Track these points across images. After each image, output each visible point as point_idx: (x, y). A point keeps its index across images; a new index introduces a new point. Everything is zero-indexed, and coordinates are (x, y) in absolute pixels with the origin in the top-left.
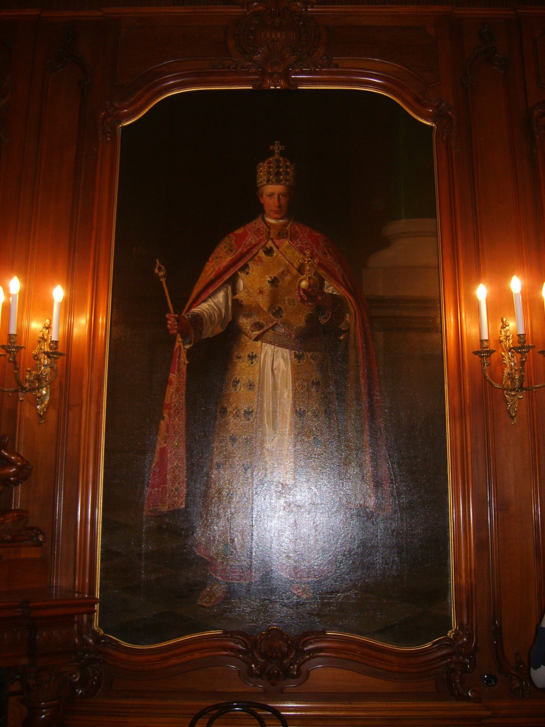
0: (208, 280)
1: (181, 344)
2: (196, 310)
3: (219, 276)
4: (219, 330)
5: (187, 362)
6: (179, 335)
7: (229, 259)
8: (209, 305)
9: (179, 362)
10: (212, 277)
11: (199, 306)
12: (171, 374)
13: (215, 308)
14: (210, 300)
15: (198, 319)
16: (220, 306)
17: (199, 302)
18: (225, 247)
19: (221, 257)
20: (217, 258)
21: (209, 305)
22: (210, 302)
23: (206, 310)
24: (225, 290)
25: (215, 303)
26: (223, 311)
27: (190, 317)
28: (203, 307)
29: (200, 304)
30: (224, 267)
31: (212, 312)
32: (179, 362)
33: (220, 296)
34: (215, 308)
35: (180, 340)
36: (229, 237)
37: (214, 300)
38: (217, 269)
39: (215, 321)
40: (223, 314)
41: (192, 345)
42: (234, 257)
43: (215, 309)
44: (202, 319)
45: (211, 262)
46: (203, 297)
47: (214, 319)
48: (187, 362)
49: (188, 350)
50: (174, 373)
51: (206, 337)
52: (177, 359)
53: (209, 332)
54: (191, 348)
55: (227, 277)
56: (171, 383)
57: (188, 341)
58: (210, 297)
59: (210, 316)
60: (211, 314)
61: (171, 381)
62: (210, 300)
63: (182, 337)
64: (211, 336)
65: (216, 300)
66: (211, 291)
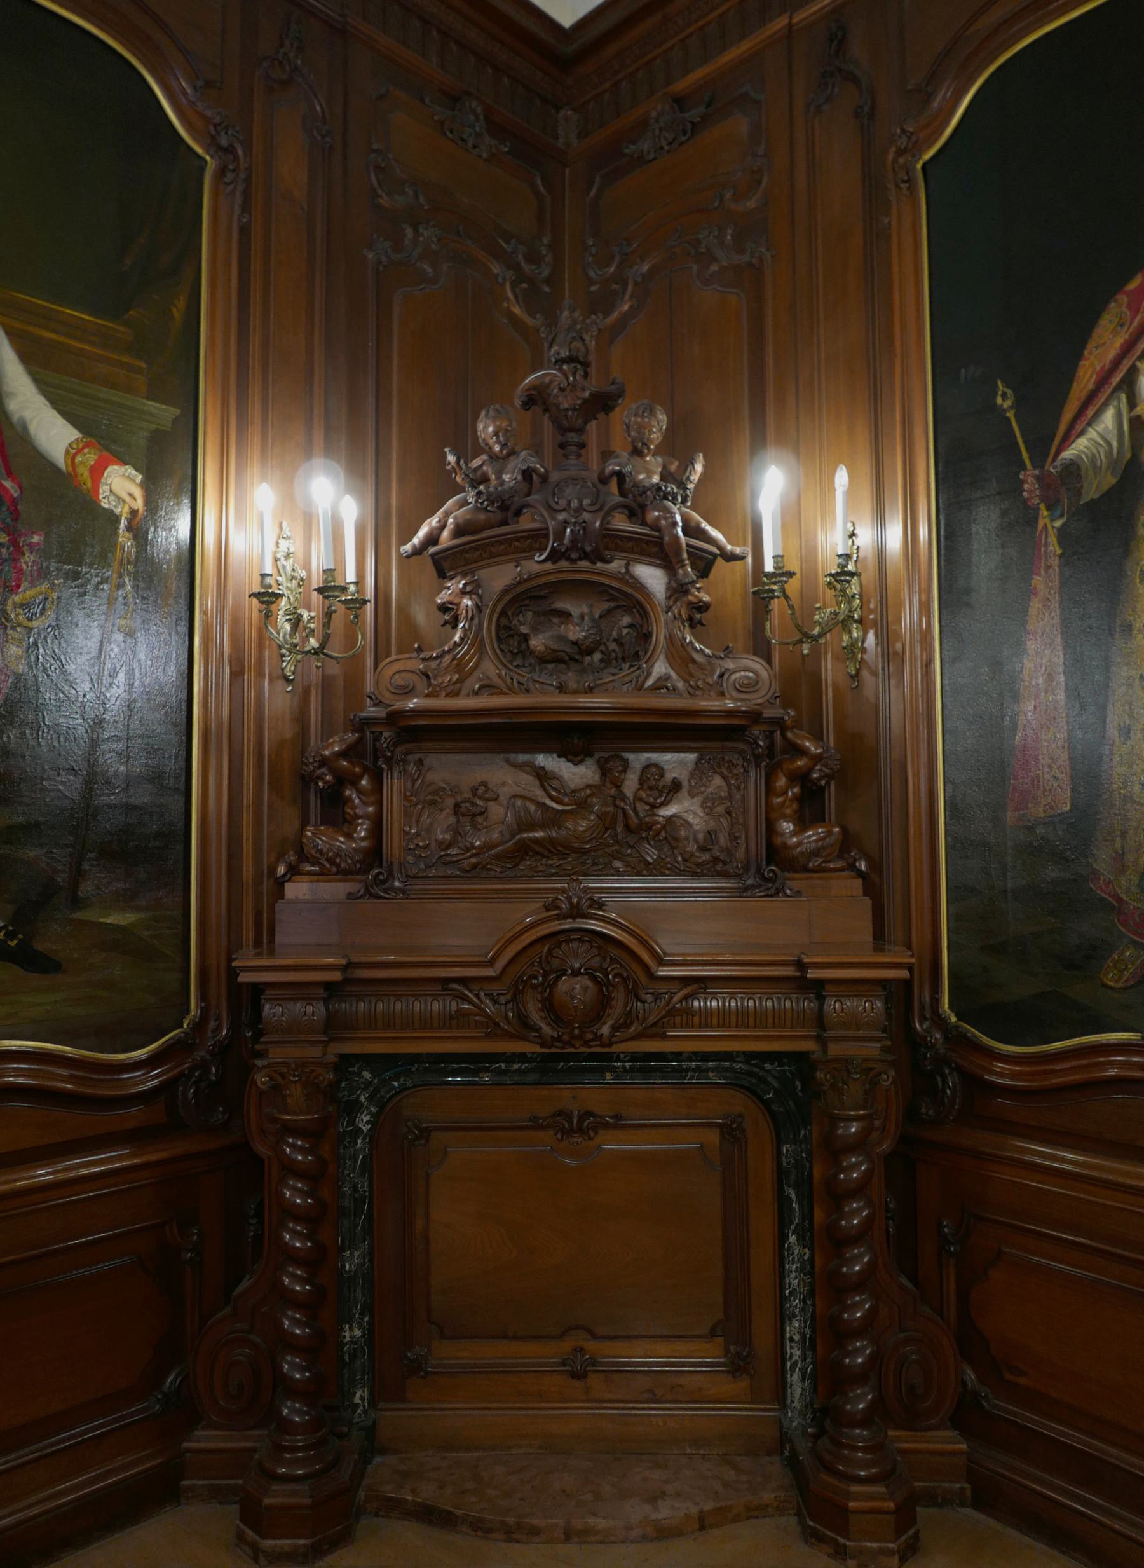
0: (1084, 395)
1: (1047, 521)
2: (1068, 454)
3: (1103, 380)
4: (1111, 480)
5: (1059, 551)
6: (1042, 506)
7: (1119, 342)
8: (1090, 440)
9: (1045, 552)
10: (1091, 386)
11: (1073, 446)
12: (1034, 577)
13: (1102, 442)
14: (1090, 429)
15: (1073, 469)
16: (1109, 437)
17: (1072, 439)
18: (1110, 322)
19: (1104, 344)
20: (1096, 348)
21: (1090, 440)
22: (1092, 433)
23: (1086, 450)
24: (1115, 403)
25: (1099, 434)
26: (1115, 444)
27: (1059, 469)
28: (1080, 447)
29: (1074, 441)
30: (1111, 362)
31: (1095, 451)
32: (1045, 552)
33: (1108, 418)
34: (1102, 442)
35: (1045, 513)
36: (1115, 301)
37: (1097, 428)
38: (1098, 368)
39: (1101, 467)
40: (1115, 450)
41: (1065, 519)
42: (1127, 337)
43: (1100, 445)
44: (1079, 468)
45: (1088, 359)
46: (1079, 428)
47: (1099, 464)
48: (1059, 551)
49: (1059, 530)
50: (1039, 574)
51: (1088, 499)
52: (1043, 549)
53: (1092, 491)
54: (1064, 525)
55: (1116, 379)
56: (1035, 593)
57: (1058, 513)
58: (1089, 424)
59: (1093, 459)
60: (1093, 455)
61: (1035, 588)
62: (1090, 429)
63: (1048, 508)
64: (1096, 496)
65: (1100, 428)
66: (1090, 412)
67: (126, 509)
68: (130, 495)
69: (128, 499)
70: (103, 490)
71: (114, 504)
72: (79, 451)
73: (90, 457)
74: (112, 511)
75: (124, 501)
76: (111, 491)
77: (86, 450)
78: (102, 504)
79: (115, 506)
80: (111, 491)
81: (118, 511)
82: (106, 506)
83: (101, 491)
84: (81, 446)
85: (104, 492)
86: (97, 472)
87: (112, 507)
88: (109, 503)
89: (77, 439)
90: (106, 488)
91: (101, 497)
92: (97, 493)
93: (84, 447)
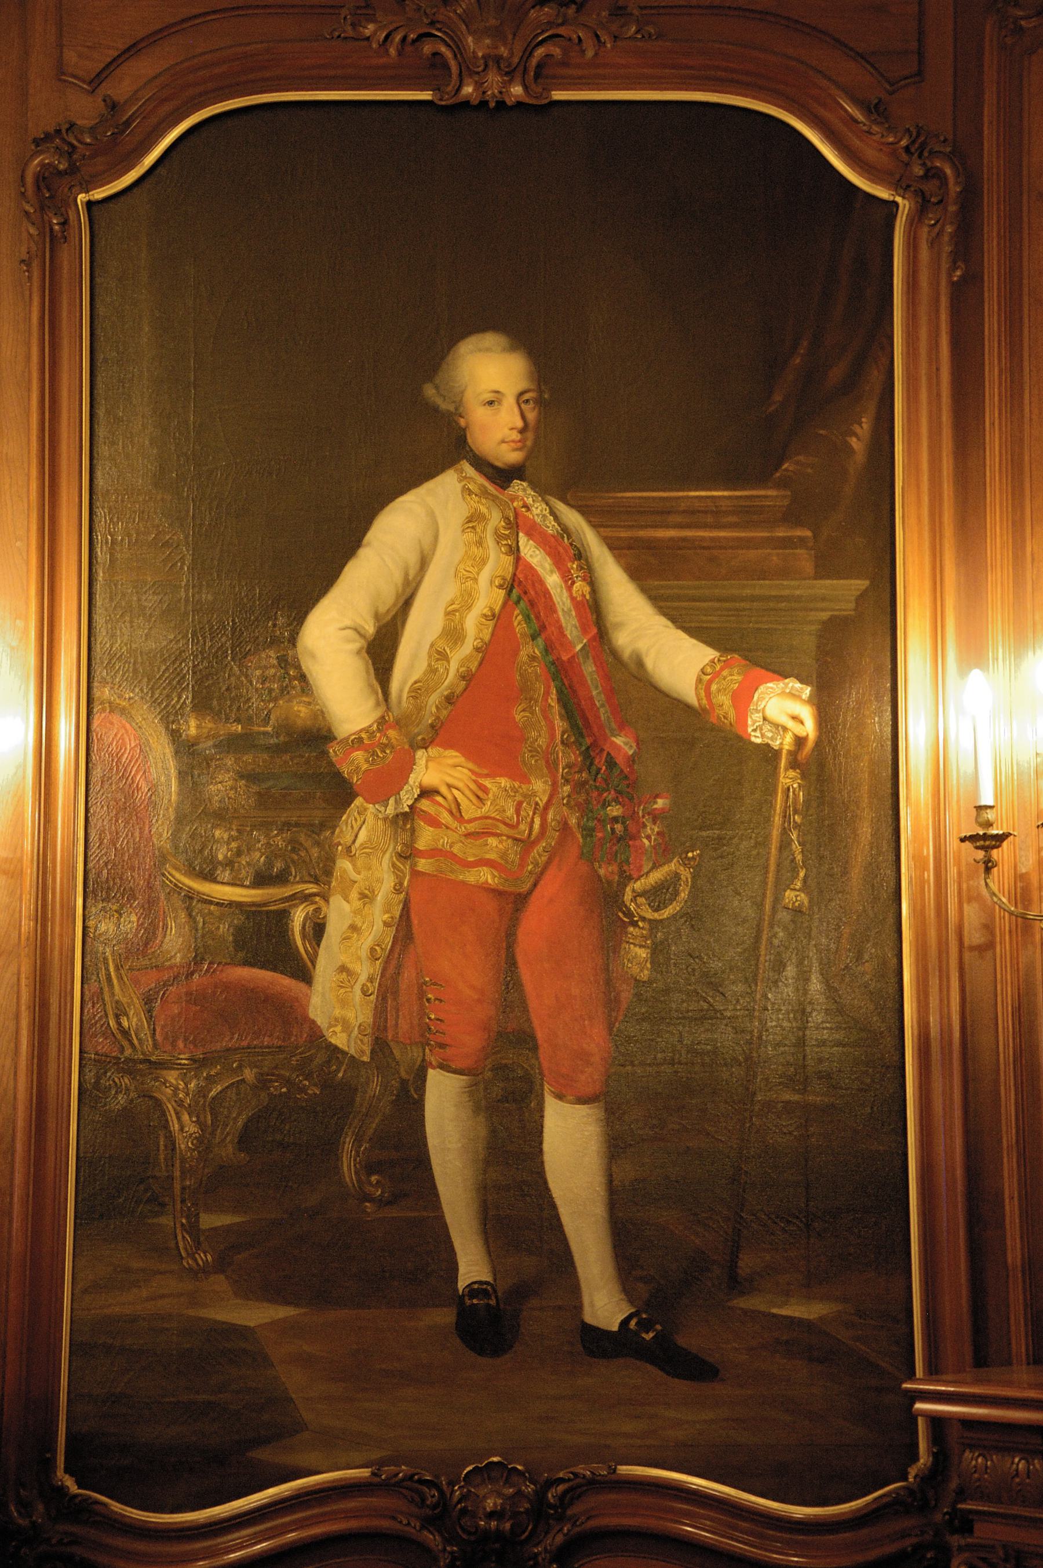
67: (789, 739)
68: (795, 718)
69: (790, 724)
70: (754, 719)
71: (770, 735)
72: (716, 675)
73: (734, 678)
74: (768, 745)
75: (785, 729)
76: (765, 719)
77: (725, 673)
78: (753, 739)
79: (772, 739)
80: (765, 719)
81: (776, 744)
82: (758, 741)
83: (750, 722)
84: (718, 668)
85: (754, 722)
86: (743, 698)
87: (766, 741)
88: (763, 735)
89: (713, 661)
90: (757, 717)
91: (750, 730)
92: (746, 725)
93: (722, 669)
